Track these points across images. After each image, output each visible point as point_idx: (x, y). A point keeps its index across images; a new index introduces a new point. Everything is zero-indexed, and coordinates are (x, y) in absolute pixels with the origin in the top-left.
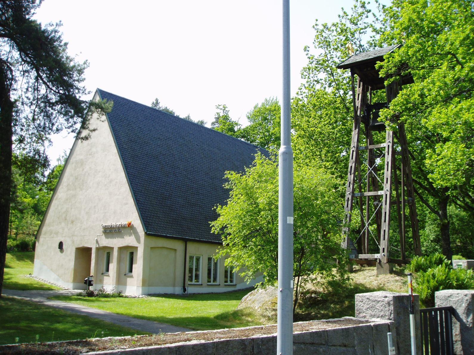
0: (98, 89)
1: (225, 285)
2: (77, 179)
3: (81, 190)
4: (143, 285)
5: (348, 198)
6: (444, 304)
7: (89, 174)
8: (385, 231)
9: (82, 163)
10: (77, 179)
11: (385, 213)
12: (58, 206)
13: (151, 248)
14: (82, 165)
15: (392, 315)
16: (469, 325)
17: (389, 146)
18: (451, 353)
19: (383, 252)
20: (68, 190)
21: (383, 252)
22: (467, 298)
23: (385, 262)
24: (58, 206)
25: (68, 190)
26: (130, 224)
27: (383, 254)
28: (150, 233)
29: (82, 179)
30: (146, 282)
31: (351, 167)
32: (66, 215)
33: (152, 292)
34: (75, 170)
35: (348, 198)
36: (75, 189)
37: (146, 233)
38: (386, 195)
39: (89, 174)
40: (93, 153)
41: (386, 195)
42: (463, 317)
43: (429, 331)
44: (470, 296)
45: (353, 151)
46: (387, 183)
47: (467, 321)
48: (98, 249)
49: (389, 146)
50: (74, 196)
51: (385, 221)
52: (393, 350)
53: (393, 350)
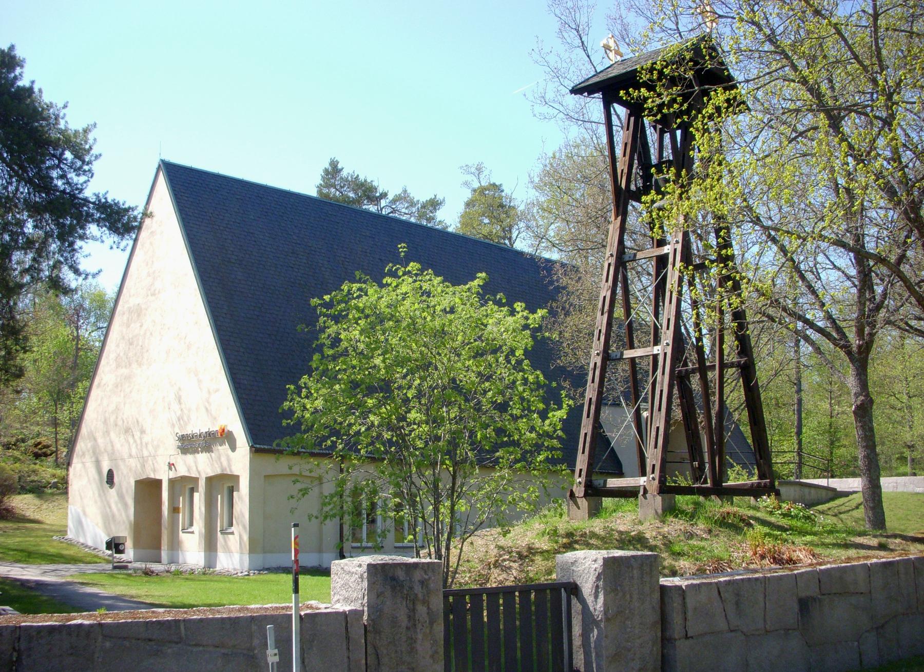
0: (163, 161)
1: (396, 547)
2: (131, 344)
3: (140, 364)
4: (252, 550)
5: (596, 363)
6: (566, 578)
7: (151, 334)
8: (658, 428)
9: (138, 312)
10: (131, 344)
11: (662, 391)
12: (102, 399)
13: (265, 476)
14: (139, 315)
15: (366, 598)
16: (598, 617)
17: (675, 250)
18: (566, 669)
19: (653, 472)
20: (118, 366)
21: (653, 472)
22: (596, 566)
23: (582, 494)
24: (102, 399)
25: (118, 366)
26: (223, 430)
27: (651, 476)
28: (262, 447)
29: (140, 344)
30: (256, 545)
31: (605, 297)
32: (117, 418)
33: (274, 565)
34: (128, 326)
35: (596, 363)
36: (130, 365)
37: (251, 447)
38: (665, 354)
39: (151, 334)
40: (157, 292)
41: (665, 354)
42: (590, 600)
43: (501, 627)
44: (601, 562)
45: (609, 265)
46: (668, 328)
47: (595, 610)
48: (172, 482)
49: (675, 250)
50: (128, 378)
51: (660, 409)
52: (275, 655)
53: (275, 655)
